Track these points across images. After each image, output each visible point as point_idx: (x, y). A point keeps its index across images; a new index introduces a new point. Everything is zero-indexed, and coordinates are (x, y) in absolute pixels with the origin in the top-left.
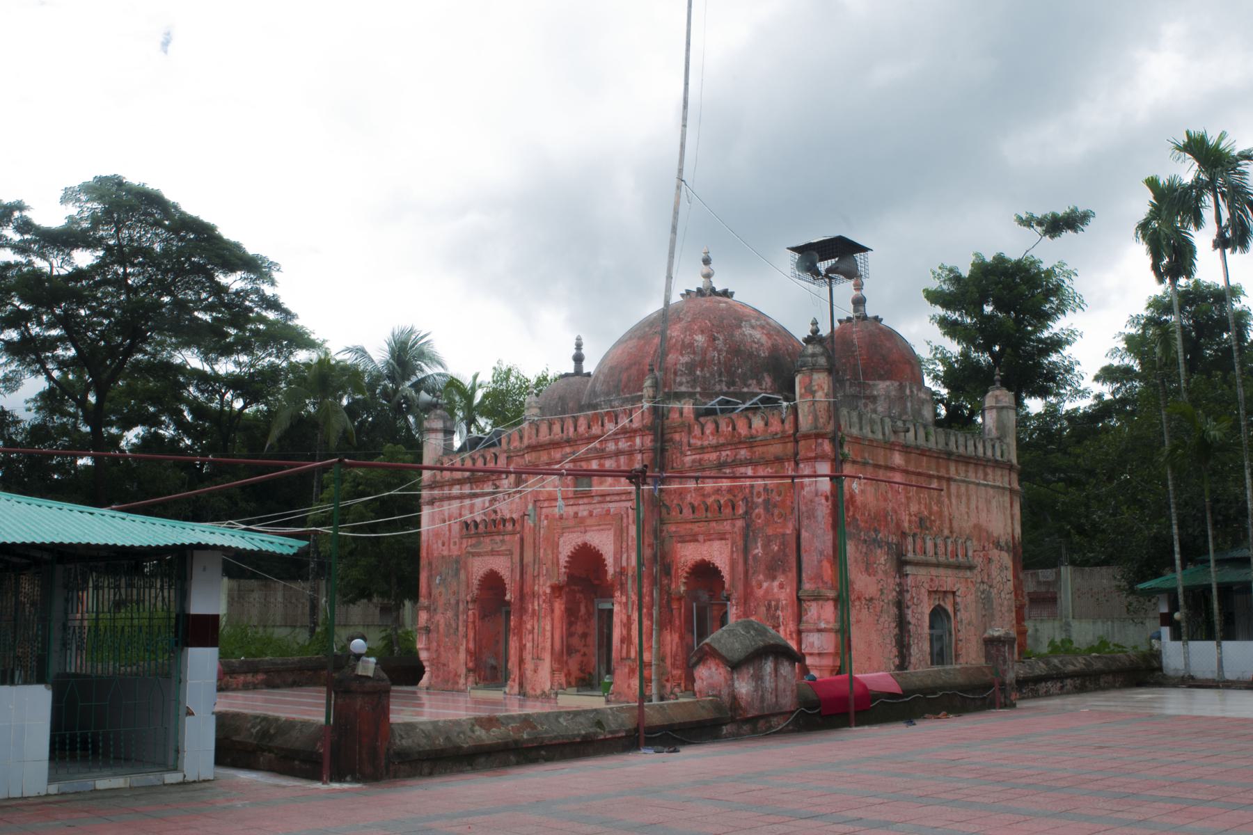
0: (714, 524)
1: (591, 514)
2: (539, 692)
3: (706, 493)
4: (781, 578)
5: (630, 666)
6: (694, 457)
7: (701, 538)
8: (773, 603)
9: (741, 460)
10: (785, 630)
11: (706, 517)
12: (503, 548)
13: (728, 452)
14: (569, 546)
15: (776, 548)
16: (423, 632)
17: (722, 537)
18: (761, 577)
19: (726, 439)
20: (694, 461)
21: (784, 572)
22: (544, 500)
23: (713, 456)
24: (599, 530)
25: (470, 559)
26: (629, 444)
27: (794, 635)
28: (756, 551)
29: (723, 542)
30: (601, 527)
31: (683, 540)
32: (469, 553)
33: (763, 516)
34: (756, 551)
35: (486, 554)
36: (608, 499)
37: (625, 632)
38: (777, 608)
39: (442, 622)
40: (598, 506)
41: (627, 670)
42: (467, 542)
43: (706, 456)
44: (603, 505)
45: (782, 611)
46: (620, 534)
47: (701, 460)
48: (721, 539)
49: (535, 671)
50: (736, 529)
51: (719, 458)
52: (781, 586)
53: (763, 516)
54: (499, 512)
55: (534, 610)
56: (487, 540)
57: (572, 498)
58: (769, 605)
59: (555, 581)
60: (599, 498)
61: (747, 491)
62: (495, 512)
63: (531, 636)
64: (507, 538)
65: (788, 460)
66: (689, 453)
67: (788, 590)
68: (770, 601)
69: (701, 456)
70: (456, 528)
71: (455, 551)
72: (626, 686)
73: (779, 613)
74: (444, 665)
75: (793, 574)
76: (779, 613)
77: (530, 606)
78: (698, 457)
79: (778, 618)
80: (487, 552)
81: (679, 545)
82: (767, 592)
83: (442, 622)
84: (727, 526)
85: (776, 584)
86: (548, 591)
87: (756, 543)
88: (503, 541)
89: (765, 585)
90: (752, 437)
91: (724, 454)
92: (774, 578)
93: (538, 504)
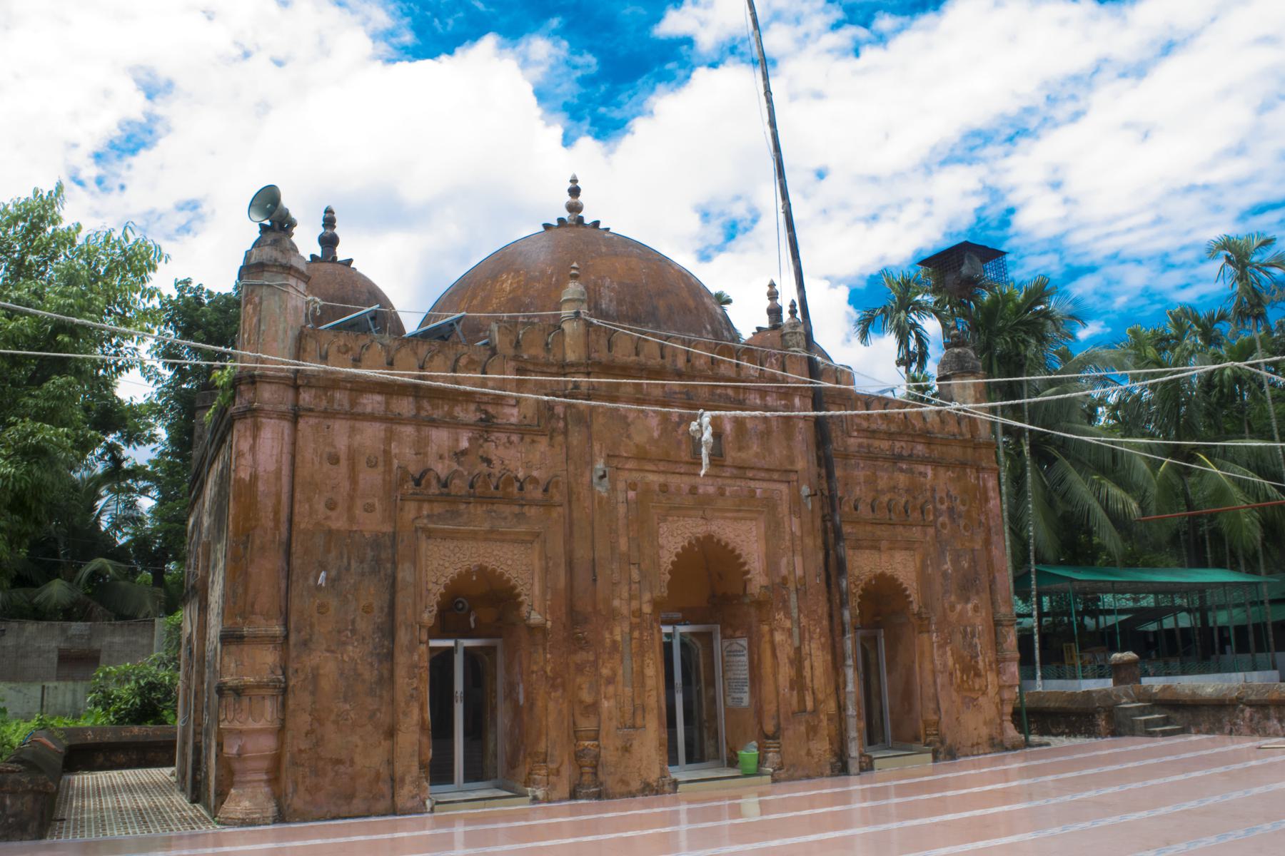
0: (901, 529)
1: (721, 492)
2: (636, 785)
3: (879, 488)
4: (975, 600)
5: (807, 722)
6: (860, 440)
7: (884, 544)
8: (969, 629)
9: (918, 456)
10: (984, 661)
11: (890, 519)
12: (522, 528)
13: (903, 444)
14: (679, 539)
15: (966, 565)
16: (270, 692)
17: (909, 546)
18: (953, 598)
19: (899, 427)
20: (860, 445)
21: (978, 593)
22: (628, 458)
23: (885, 445)
24: (735, 519)
25: (425, 546)
26: (783, 402)
27: (994, 666)
28: (946, 567)
29: (908, 552)
30: (741, 515)
31: (858, 546)
32: (425, 530)
33: (948, 527)
34: (946, 567)
35: (474, 536)
36: (750, 474)
37: (793, 673)
38: (973, 636)
39: (330, 668)
40: (729, 481)
41: (803, 729)
42: (420, 509)
43: (876, 443)
44: (738, 482)
45: (979, 638)
46: (774, 529)
47: (869, 446)
48: (906, 549)
49: (626, 749)
50: (928, 538)
51: (892, 448)
52: (976, 609)
53: (948, 527)
54: (496, 462)
55: (614, 642)
56: (480, 510)
57: (687, 463)
58: (965, 631)
59: (657, 593)
60: (735, 471)
61: (928, 494)
62: (488, 461)
63: (611, 689)
64: (532, 512)
65: (972, 467)
66: (855, 434)
67: (984, 614)
68: (966, 627)
69: (870, 441)
70: (371, 478)
71: (373, 523)
72: (803, 753)
73: (976, 640)
74: (339, 762)
75: (986, 596)
76: (976, 640)
77: (607, 635)
78: (865, 441)
79: (976, 646)
80: (475, 532)
81: (851, 552)
82: (961, 614)
83: (330, 668)
84: (916, 533)
85: (970, 606)
86: (647, 609)
87: (945, 557)
88: (520, 517)
89: (959, 607)
90: (928, 432)
91: (898, 444)
92: (967, 600)
93: (615, 462)
